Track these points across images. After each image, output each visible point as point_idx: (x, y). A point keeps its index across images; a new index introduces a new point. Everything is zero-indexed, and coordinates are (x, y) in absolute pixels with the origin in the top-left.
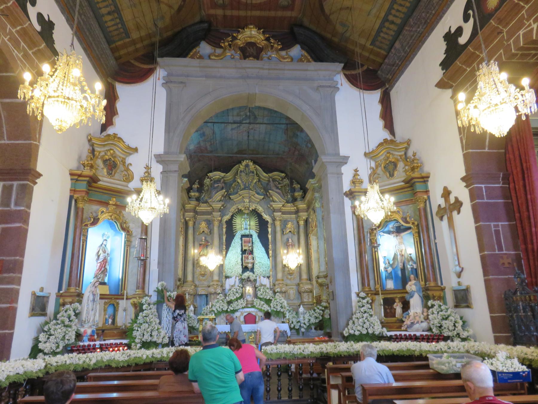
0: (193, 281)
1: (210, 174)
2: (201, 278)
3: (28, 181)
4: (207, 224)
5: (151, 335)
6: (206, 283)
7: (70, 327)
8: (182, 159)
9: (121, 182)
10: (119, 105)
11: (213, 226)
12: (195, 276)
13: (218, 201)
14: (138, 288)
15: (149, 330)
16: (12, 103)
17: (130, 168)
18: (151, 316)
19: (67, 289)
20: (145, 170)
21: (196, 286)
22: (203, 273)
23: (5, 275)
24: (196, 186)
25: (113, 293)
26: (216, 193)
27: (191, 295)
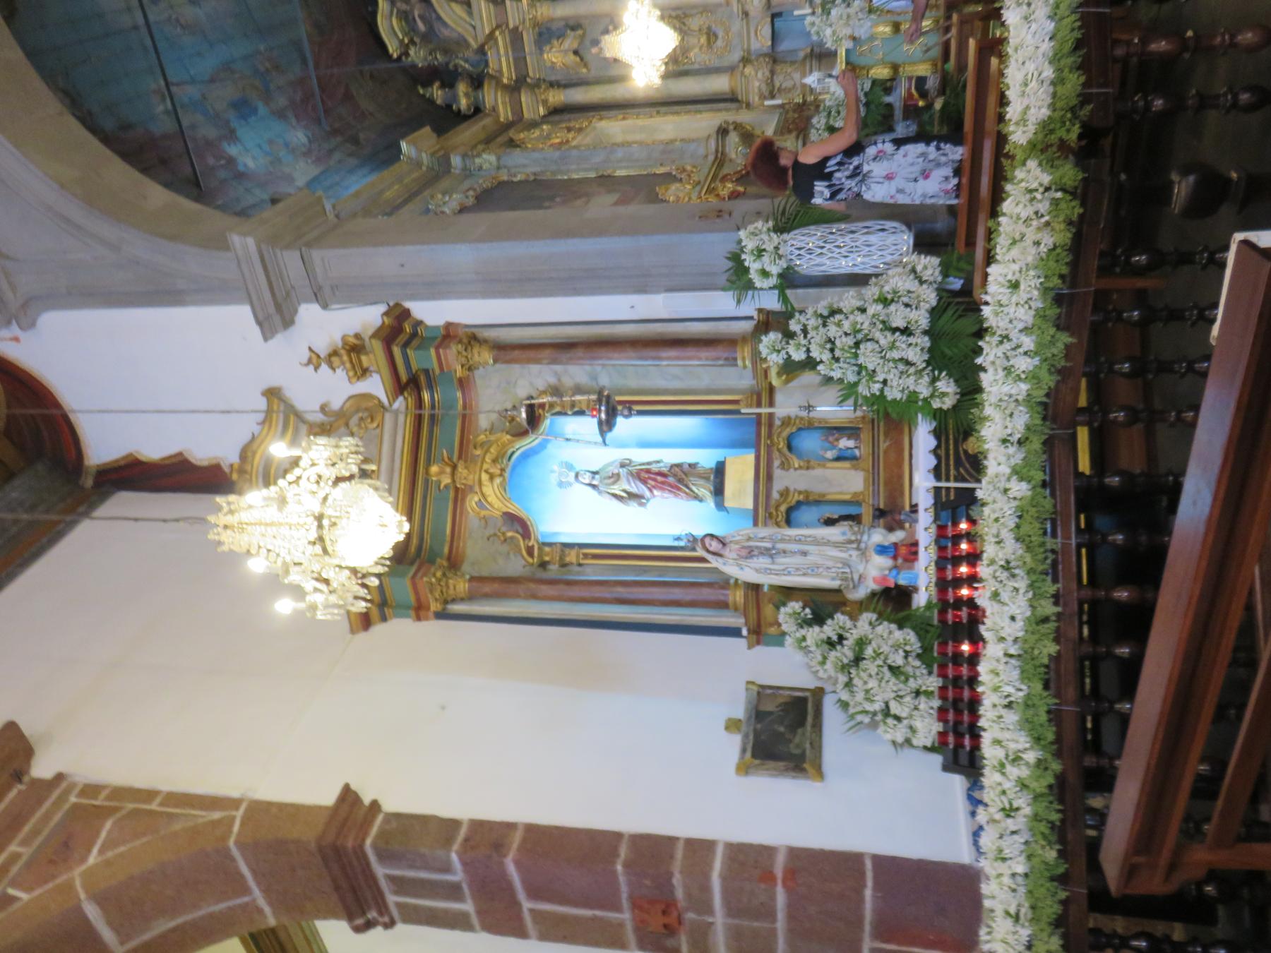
0: (731, 69)
1: (393, 48)
2: (719, 43)
3: (361, 847)
4: (549, 42)
5: (906, 331)
6: (737, 25)
7: (862, 643)
8: (250, 241)
9: (387, 437)
10: (154, 450)
11: (552, 20)
12: (715, 62)
13: (470, 14)
14: (732, 362)
15: (883, 342)
16: (110, 924)
17: (336, 404)
18: (833, 331)
19: (736, 609)
20: (324, 367)
21: (746, 60)
22: (703, 40)
23: (679, 893)
24: (437, 94)
25: (753, 436)
26: (445, 24)
27: (772, 72)
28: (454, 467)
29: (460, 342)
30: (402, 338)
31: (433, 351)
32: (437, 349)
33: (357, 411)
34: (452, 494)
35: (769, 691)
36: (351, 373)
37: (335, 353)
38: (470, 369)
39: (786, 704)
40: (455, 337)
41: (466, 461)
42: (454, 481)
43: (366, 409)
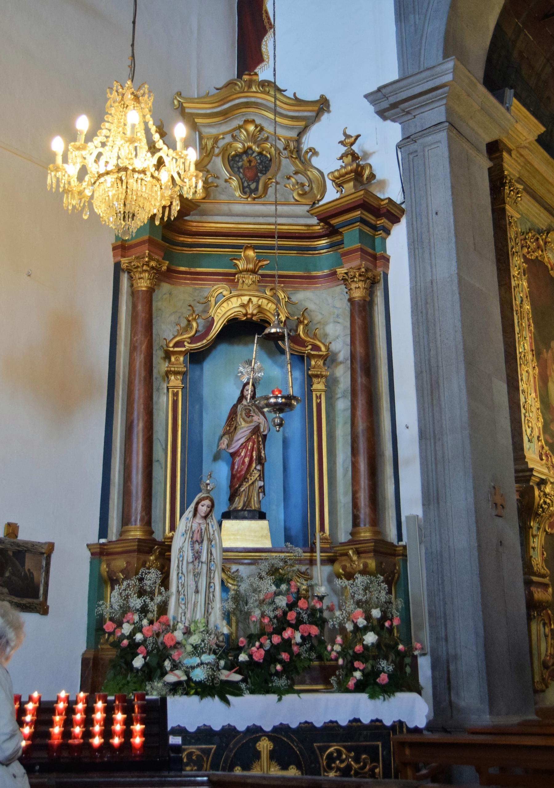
20: (343, 149)
28: (254, 272)
29: (367, 270)
30: (370, 218)
31: (358, 245)
32: (362, 250)
33: (310, 181)
34: (233, 271)
35: (44, 563)
36: (336, 174)
37: (355, 157)
38: (344, 280)
39: (33, 578)
40: (375, 266)
41: (259, 282)
42: (241, 272)
43: (312, 189)
